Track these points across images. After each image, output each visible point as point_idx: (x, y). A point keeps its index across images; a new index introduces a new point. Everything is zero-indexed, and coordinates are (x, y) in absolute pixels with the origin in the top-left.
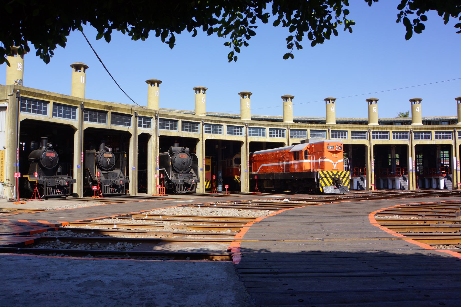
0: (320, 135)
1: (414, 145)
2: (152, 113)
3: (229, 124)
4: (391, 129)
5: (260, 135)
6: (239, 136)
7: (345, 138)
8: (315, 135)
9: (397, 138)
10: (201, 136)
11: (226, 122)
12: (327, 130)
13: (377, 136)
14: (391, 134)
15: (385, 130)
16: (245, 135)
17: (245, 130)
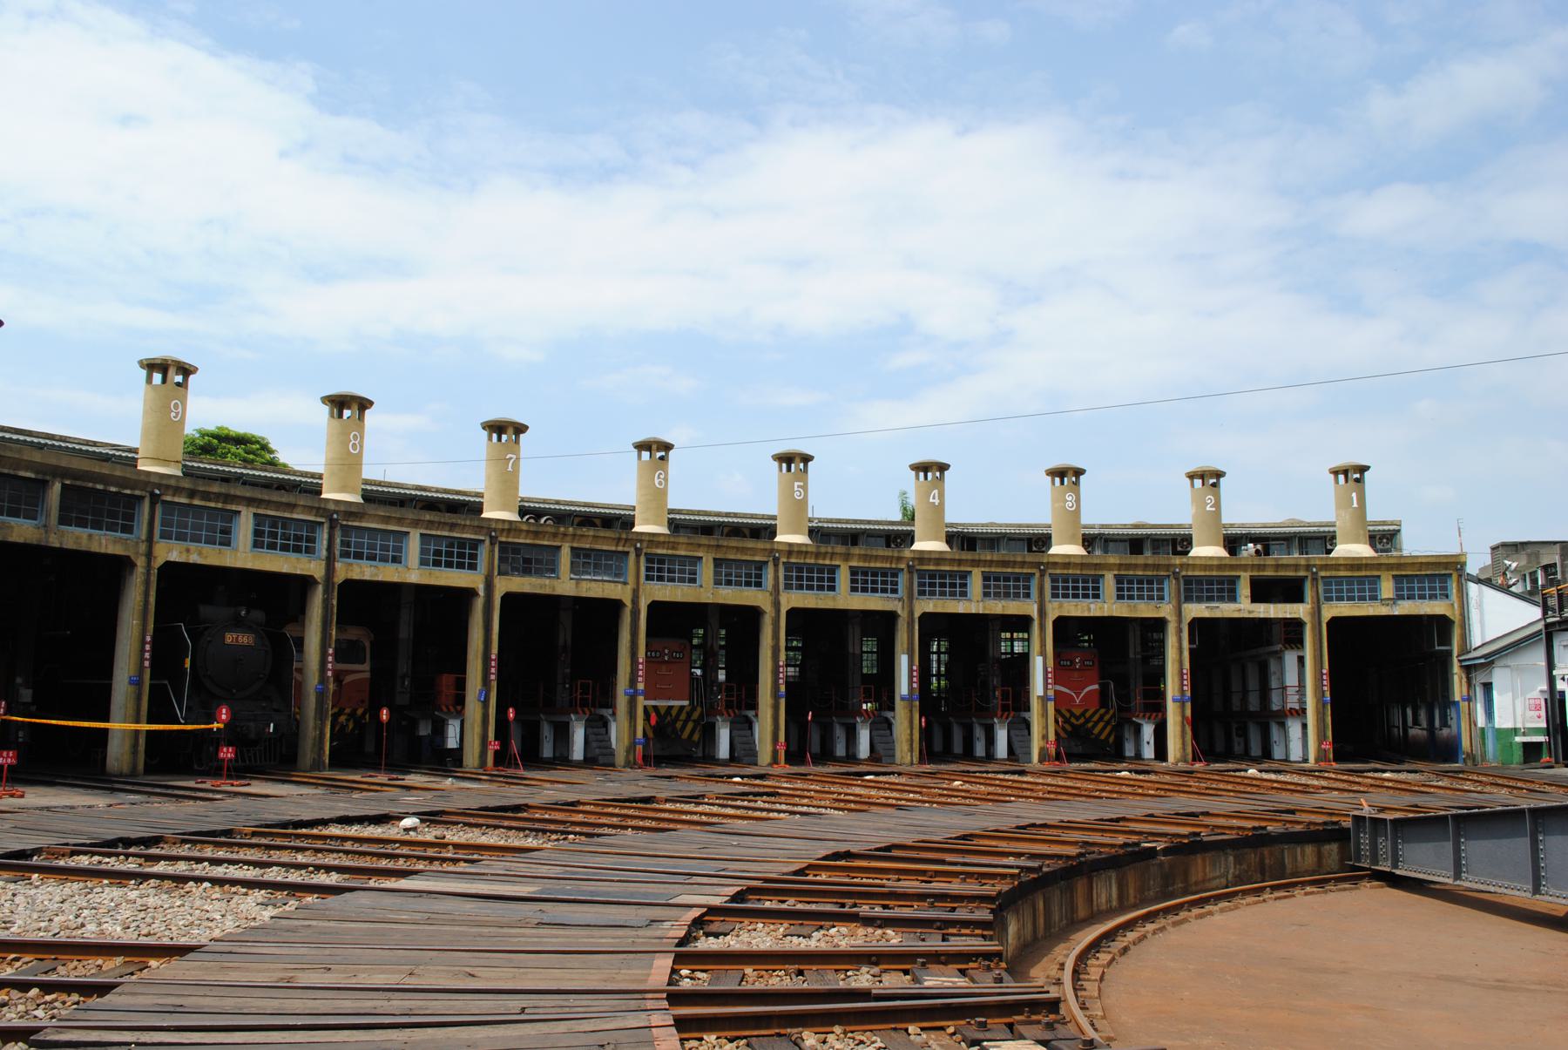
1: (917, 615)
3: (261, 511)
4: (847, 557)
5: (384, 559)
6: (303, 558)
7: (693, 581)
9: (864, 590)
10: (143, 548)
11: (250, 502)
12: (632, 550)
13: (799, 578)
14: (843, 578)
16: (324, 553)
17: (326, 536)
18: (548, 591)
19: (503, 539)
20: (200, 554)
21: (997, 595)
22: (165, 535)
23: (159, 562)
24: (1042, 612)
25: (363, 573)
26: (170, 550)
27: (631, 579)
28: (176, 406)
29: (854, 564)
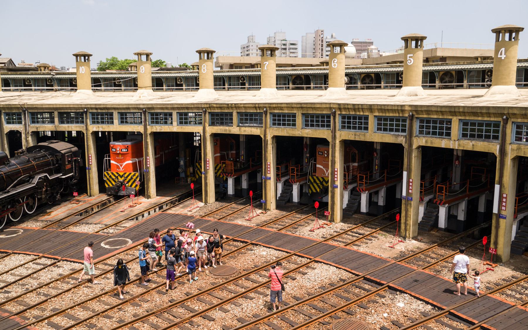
0: (256, 120)
2: (18, 108)
3: (120, 111)
8: (246, 119)
10: (85, 127)
13: (349, 123)
15: (362, 113)
18: (228, 132)
19: (210, 111)
20: (102, 128)
21: (472, 136)
22: (94, 123)
23: (91, 131)
24: (503, 151)
26: (93, 128)
27: (264, 125)
28: (142, 68)
29: (377, 114)
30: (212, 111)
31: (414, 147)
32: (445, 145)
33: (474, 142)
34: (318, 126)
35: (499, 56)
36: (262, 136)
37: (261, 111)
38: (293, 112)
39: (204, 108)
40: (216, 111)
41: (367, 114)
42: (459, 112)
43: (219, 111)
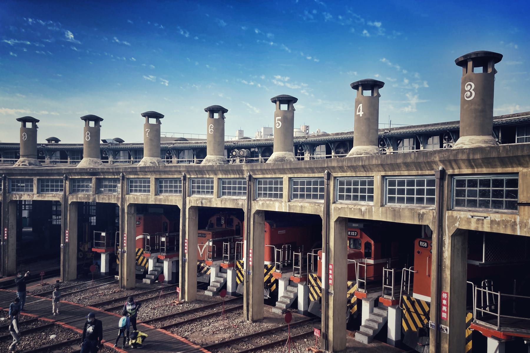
1: (253, 211)
15: (208, 176)
25: (16, 197)
29: (220, 176)
30: (73, 177)
31: (253, 211)
32: (278, 208)
33: (302, 204)
34: (171, 191)
35: (358, 113)
36: (119, 204)
37: (119, 177)
38: (147, 176)
39: (65, 173)
40: (77, 177)
41: (212, 176)
42: (287, 169)
43: (79, 177)
